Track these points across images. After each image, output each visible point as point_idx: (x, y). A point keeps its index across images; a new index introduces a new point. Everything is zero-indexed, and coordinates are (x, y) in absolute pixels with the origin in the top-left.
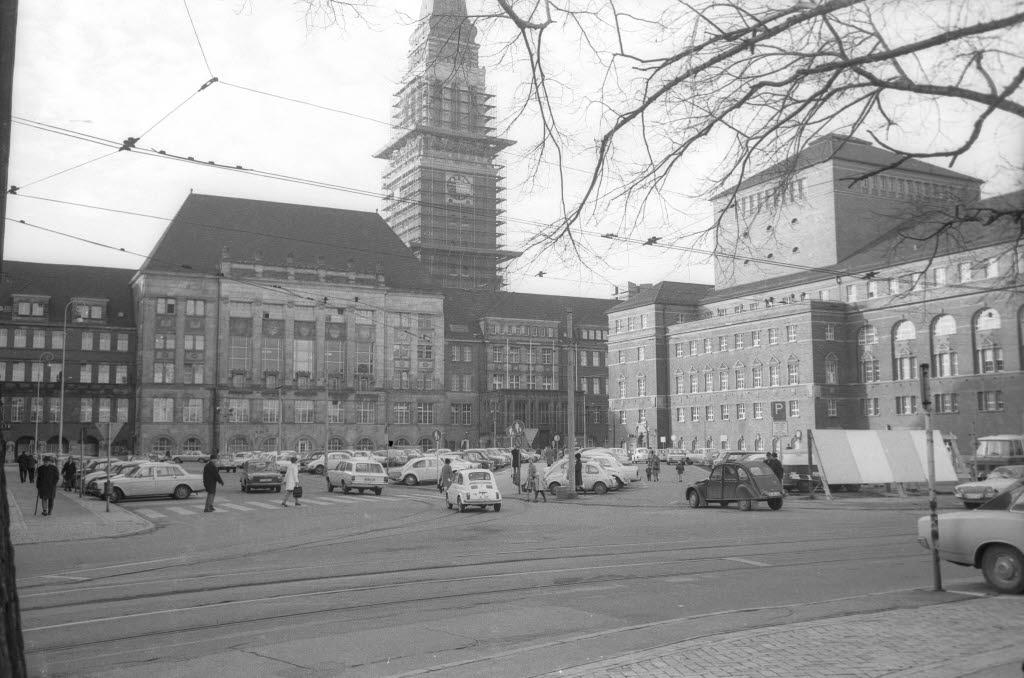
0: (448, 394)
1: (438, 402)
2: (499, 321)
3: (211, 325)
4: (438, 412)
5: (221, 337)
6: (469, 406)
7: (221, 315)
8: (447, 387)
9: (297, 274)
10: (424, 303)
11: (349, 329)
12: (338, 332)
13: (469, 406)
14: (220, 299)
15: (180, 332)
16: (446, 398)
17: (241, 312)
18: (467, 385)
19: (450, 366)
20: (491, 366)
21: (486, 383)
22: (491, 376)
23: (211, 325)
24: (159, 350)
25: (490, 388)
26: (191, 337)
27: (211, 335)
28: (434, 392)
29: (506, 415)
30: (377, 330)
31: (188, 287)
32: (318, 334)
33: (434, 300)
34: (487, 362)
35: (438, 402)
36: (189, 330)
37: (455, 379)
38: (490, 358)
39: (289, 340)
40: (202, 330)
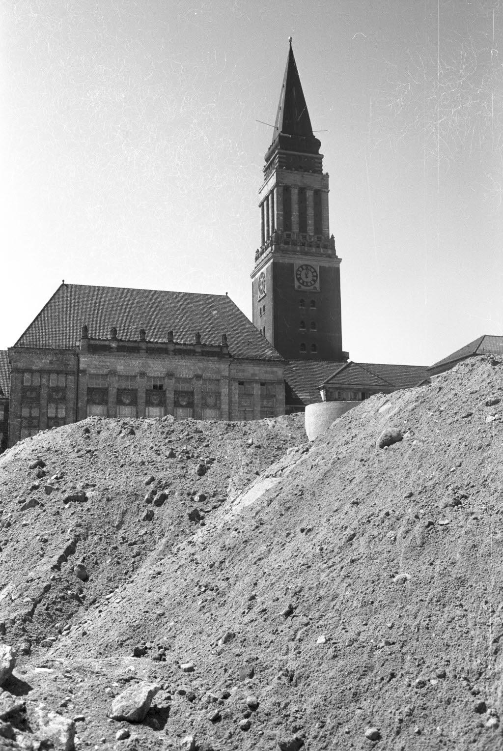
2: (337, 388)
3: (71, 395)
5: (80, 404)
7: (81, 386)
9: (147, 348)
10: (266, 372)
11: (196, 397)
12: (186, 399)
14: (78, 372)
15: (43, 402)
17: (95, 384)
23: (71, 395)
24: (25, 418)
26: (53, 405)
27: (71, 405)
30: (222, 398)
31: (51, 363)
32: (168, 401)
33: (275, 369)
36: (50, 399)
39: (141, 407)
40: (64, 399)
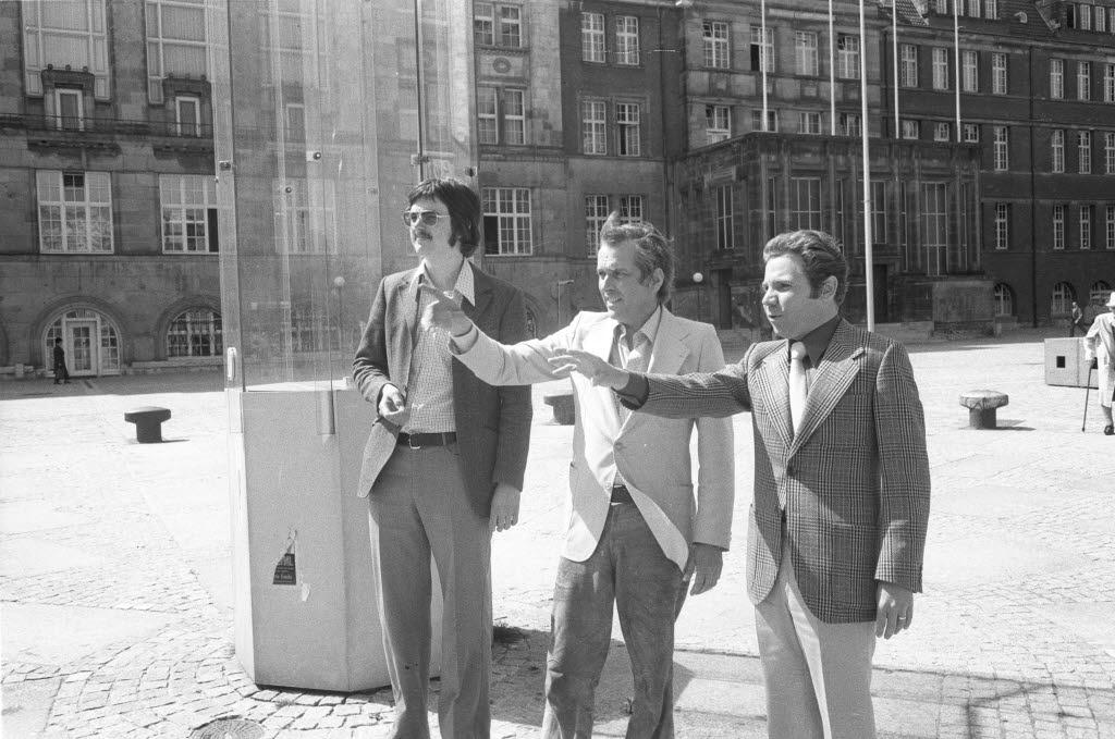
0: (577, 164)
1: (545, 183)
4: (549, 215)
6: (635, 201)
8: (569, 144)
13: (635, 201)
16: (570, 174)
18: (634, 140)
19: (578, 76)
20: (698, 80)
21: (686, 133)
22: (698, 111)
25: (695, 142)
28: (534, 152)
29: (765, 218)
34: (684, 68)
35: (545, 183)
37: (593, 118)
38: (693, 51)
